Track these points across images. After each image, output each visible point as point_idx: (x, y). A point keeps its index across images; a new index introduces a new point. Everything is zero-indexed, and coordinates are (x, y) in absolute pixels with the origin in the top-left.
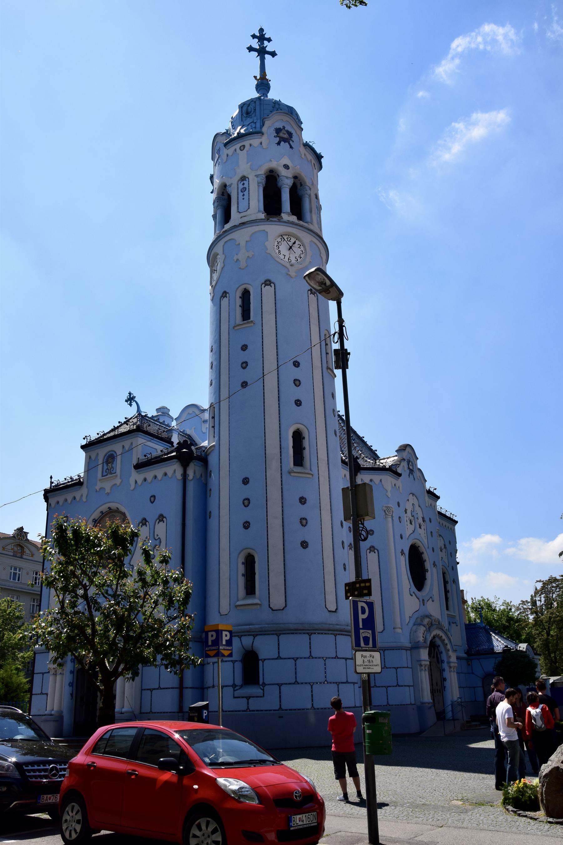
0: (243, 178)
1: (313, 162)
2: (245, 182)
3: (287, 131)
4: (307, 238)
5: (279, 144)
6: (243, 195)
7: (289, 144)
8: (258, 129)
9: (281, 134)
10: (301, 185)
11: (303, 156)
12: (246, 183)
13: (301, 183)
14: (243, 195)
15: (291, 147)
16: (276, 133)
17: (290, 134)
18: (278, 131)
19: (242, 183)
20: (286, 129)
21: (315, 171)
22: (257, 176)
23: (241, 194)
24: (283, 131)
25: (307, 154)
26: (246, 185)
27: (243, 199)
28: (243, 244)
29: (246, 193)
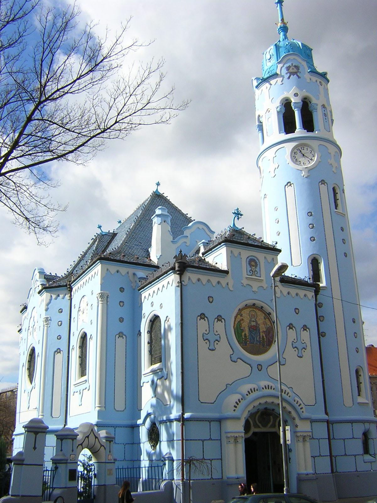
0: (268, 111)
1: (319, 80)
3: (295, 66)
4: (315, 144)
5: (289, 78)
7: (297, 75)
9: (291, 70)
10: (310, 103)
11: (308, 81)
13: (310, 101)
15: (299, 77)
16: (287, 70)
17: (297, 67)
18: (288, 68)
20: (294, 65)
21: (321, 88)
24: (291, 68)
25: (312, 77)
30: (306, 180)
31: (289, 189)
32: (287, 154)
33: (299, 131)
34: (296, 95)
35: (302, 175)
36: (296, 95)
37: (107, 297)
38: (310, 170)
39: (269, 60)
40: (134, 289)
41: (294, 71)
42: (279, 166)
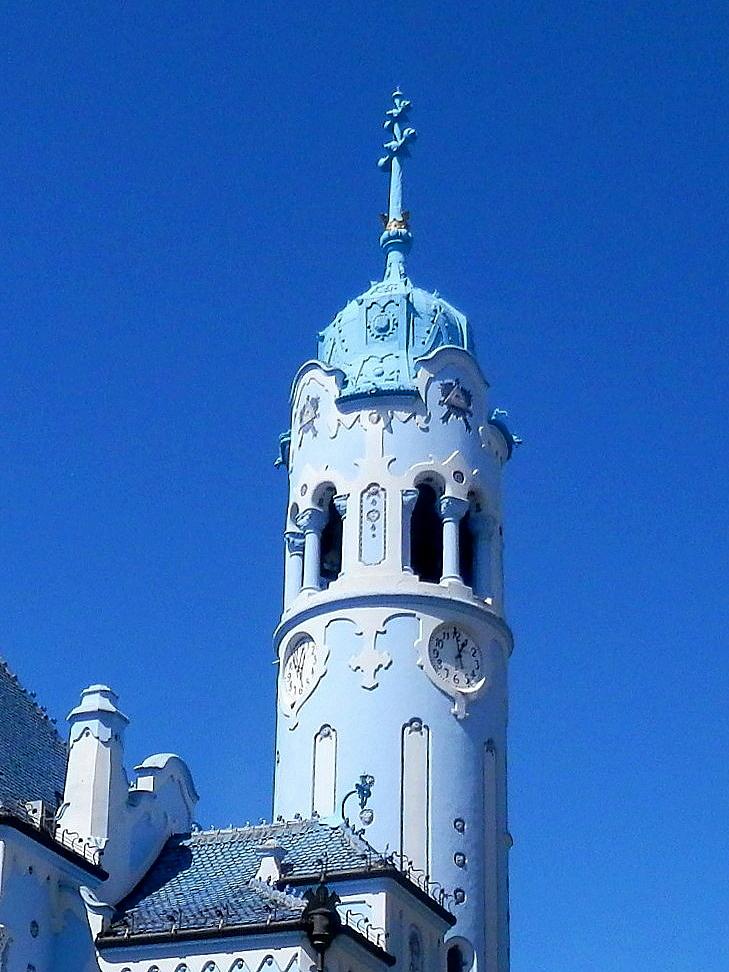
0: (373, 489)
2: (375, 497)
5: (445, 418)
6: (373, 528)
7: (465, 420)
8: (408, 384)
12: (380, 500)
14: (373, 528)
15: (468, 427)
18: (446, 389)
19: (372, 498)
22: (405, 493)
23: (367, 525)
26: (379, 507)
27: (374, 536)
28: (369, 635)
29: (380, 523)
30: (459, 730)
31: (411, 737)
32: (420, 639)
33: (450, 583)
34: (458, 476)
35: (453, 711)
36: (458, 476)
37: (7, 946)
38: (472, 703)
39: (381, 330)
40: (56, 935)
41: (461, 405)
42: (391, 663)
